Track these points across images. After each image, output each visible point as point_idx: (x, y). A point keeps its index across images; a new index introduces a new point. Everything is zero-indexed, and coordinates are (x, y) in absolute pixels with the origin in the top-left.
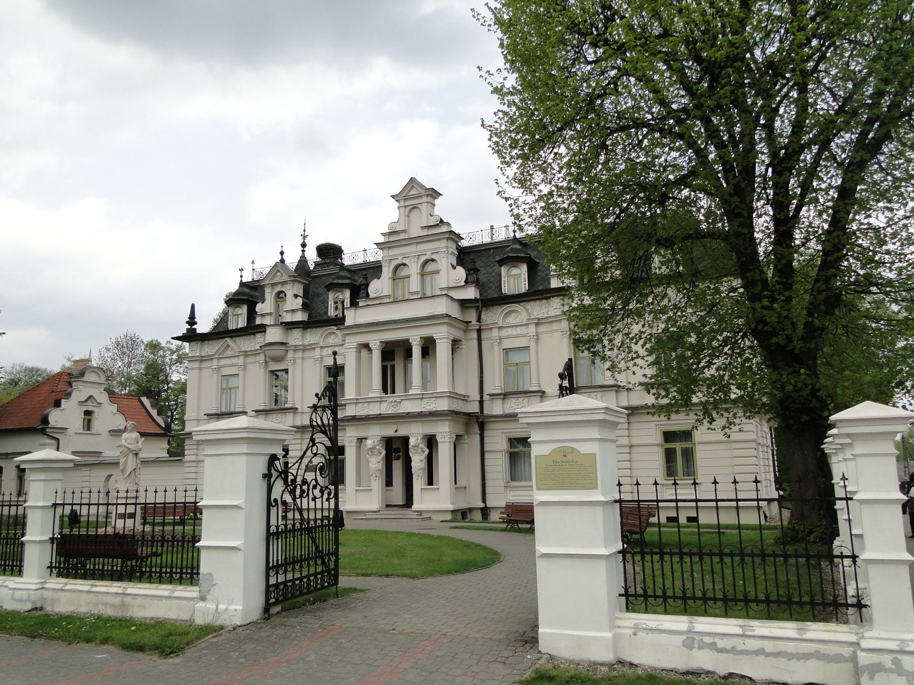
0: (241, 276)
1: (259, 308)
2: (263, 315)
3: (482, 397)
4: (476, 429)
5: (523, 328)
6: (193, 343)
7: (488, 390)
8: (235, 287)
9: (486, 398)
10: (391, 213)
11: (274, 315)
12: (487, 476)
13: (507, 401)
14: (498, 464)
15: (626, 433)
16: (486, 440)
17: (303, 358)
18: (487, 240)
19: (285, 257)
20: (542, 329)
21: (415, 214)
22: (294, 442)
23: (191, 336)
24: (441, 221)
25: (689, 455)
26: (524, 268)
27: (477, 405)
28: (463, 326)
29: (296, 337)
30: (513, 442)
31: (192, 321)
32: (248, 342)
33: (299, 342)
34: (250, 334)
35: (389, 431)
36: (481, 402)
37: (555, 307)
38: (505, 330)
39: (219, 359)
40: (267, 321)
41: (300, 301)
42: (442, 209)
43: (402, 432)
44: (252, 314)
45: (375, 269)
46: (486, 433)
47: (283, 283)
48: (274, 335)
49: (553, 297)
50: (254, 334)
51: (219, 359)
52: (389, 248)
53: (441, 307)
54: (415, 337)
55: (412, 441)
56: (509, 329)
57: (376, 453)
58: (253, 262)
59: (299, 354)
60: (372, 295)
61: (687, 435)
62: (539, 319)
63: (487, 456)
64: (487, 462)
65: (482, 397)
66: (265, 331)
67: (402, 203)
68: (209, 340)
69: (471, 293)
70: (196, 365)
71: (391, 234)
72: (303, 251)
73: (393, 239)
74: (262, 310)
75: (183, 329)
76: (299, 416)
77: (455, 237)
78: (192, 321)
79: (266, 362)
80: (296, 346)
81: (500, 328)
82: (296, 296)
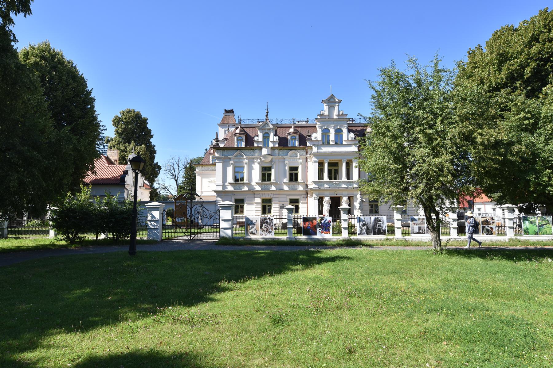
22: (275, 196)
40: (261, 145)
48: (265, 151)
78: (217, 140)
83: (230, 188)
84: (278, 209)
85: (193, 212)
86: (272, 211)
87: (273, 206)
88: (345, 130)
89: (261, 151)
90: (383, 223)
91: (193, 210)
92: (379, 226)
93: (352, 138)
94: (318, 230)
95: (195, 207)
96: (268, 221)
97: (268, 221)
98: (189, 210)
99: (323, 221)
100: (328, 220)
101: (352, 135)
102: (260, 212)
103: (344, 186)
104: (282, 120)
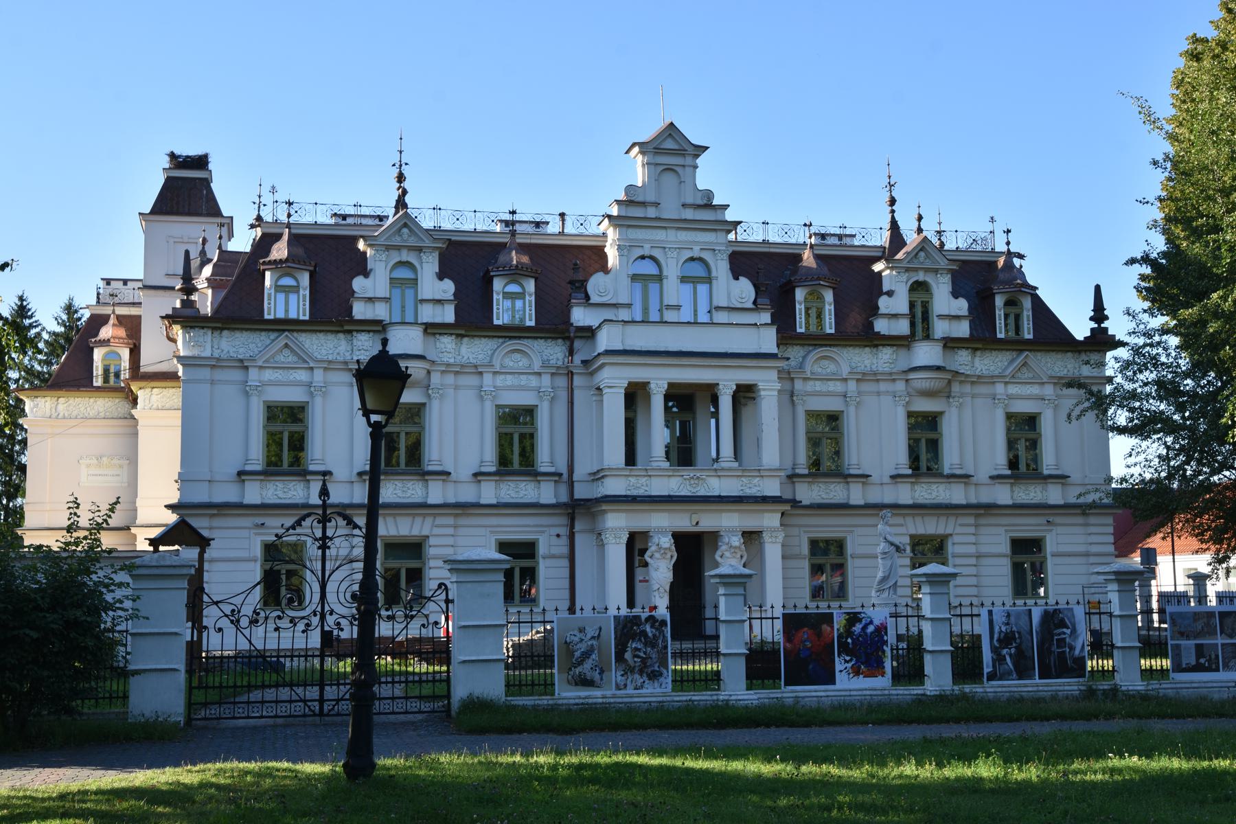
2: (370, 300)
5: (838, 383)
10: (637, 171)
17: (456, 388)
20: (866, 387)
21: (669, 179)
22: (436, 531)
35: (683, 521)
37: (884, 359)
38: (811, 383)
40: (380, 312)
43: (708, 521)
49: (884, 345)
51: (261, 367)
52: (629, 226)
54: (727, 380)
57: (669, 556)
59: (450, 379)
60: (594, 299)
70: (205, 373)
76: (450, 486)
80: (448, 365)
85: (331, 597)
90: (1074, 631)
91: (331, 587)
92: (1061, 642)
94: (841, 664)
95: (338, 575)
96: (648, 628)
97: (648, 628)
98: (316, 588)
99: (857, 628)
100: (877, 622)
101: (744, 290)
104: (458, 215)
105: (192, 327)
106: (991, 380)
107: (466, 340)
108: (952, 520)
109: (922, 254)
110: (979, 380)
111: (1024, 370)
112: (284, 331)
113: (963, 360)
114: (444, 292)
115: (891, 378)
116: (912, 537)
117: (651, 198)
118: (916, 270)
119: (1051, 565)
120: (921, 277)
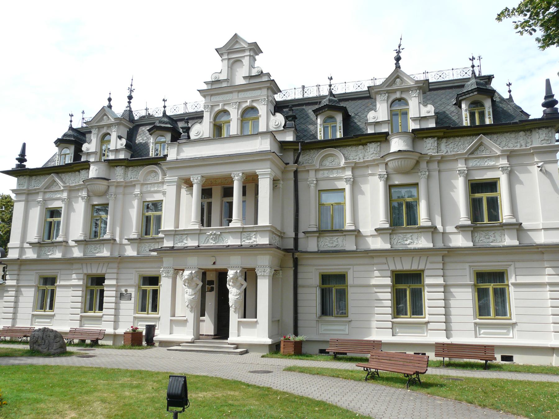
0: (71, 121)
1: (85, 147)
2: (88, 154)
3: (297, 235)
4: (291, 264)
6: (21, 178)
7: (303, 227)
8: (65, 130)
9: (301, 235)
11: (99, 154)
12: (300, 310)
13: (321, 239)
14: (311, 299)
15: (441, 272)
16: (300, 276)
17: (124, 194)
18: (299, 96)
19: (112, 103)
22: (109, 271)
23: (20, 171)
24: (262, 72)
25: (501, 295)
26: (339, 118)
27: (292, 241)
28: (282, 165)
29: (119, 174)
30: (325, 278)
31: (22, 158)
32: (72, 179)
33: (120, 179)
34: (75, 171)
35: (208, 264)
36: (296, 239)
37: (371, 152)
38: (321, 172)
39: (45, 193)
41: (124, 141)
42: (263, 63)
44: (78, 153)
45: (198, 117)
46: (300, 269)
47: (109, 126)
49: (370, 142)
50: (79, 171)
52: (212, 95)
53: (264, 145)
55: (231, 273)
56: (326, 172)
58: (83, 112)
59: (121, 190)
61: (499, 276)
62: (356, 163)
63: (300, 290)
64: (300, 297)
65: (297, 235)
66: (88, 169)
67: (225, 57)
68: (36, 175)
69: (290, 137)
70: (23, 197)
71: (213, 83)
72: (129, 103)
73: (214, 89)
74: (88, 149)
75: (13, 164)
77: (274, 88)
78: (22, 158)
79: (88, 196)
80: (118, 182)
81: (316, 170)
82: (120, 137)
83: (30, 254)
84: (113, 299)
86: (105, 305)
87: (105, 293)
88: (263, 109)
89: (88, 173)
93: (278, 126)
101: (280, 119)
102: (79, 305)
103: (231, 241)
105: (20, 176)
106: (455, 159)
107: (130, 168)
108: (423, 260)
109: (398, 80)
110: (442, 160)
111: (482, 148)
112: (50, 174)
113: (429, 147)
114: (122, 145)
115: (374, 164)
116: (393, 272)
117: (223, 76)
118: (395, 91)
119: (513, 294)
120: (398, 95)
